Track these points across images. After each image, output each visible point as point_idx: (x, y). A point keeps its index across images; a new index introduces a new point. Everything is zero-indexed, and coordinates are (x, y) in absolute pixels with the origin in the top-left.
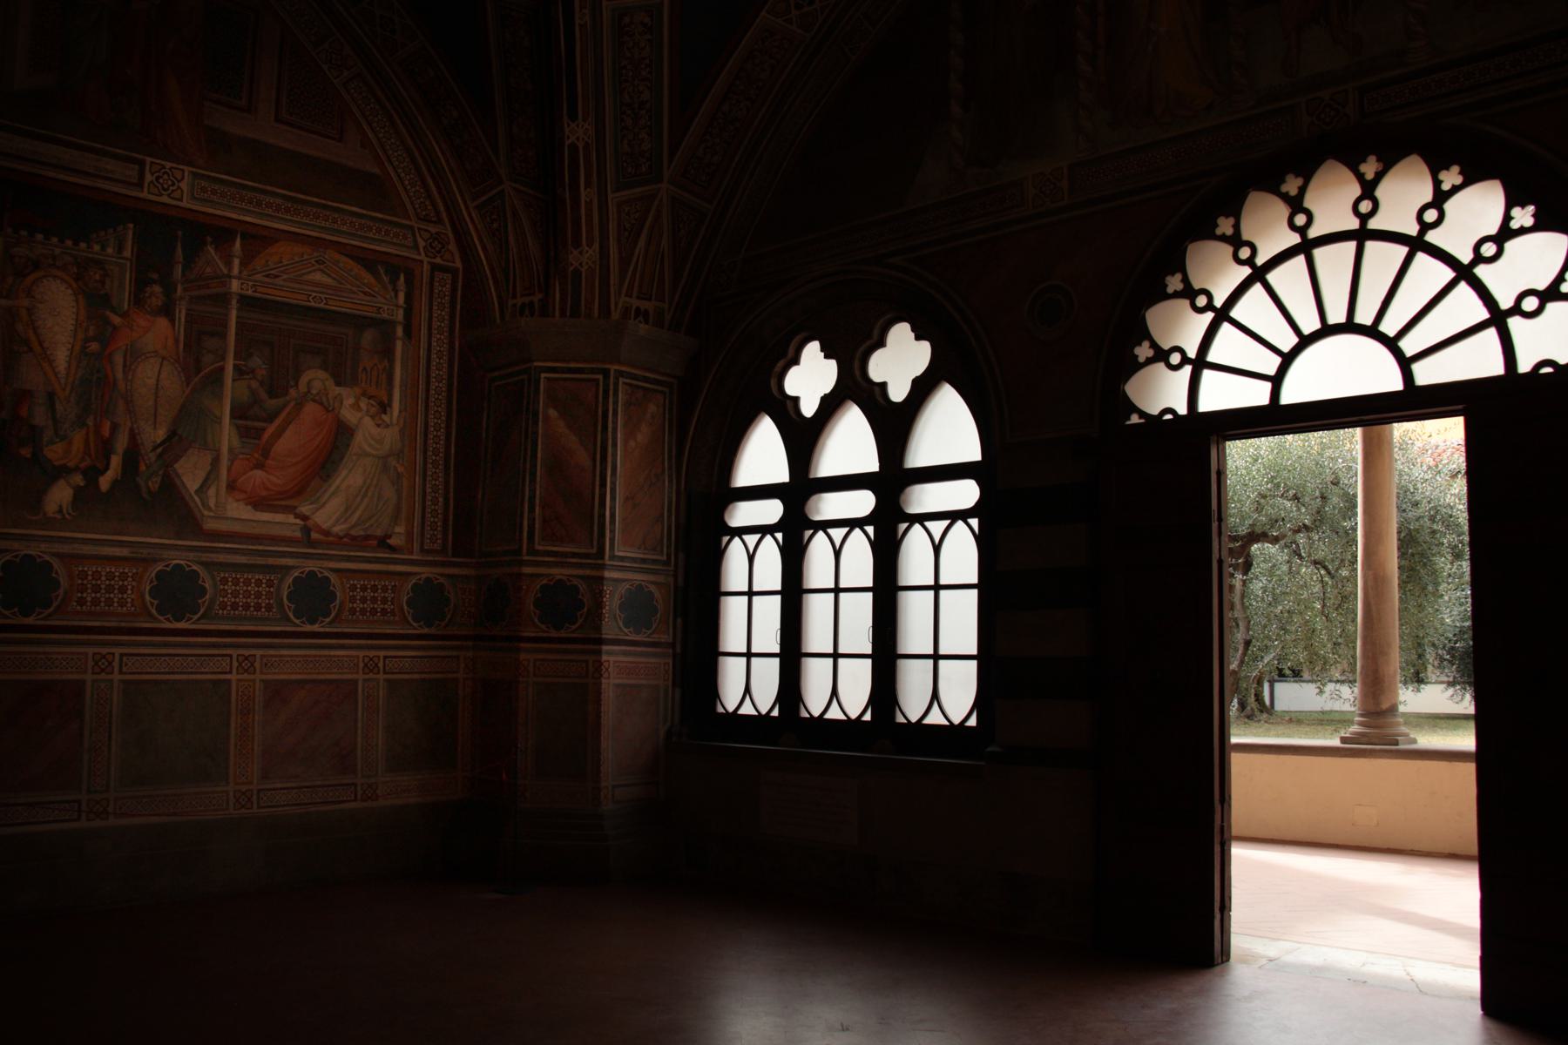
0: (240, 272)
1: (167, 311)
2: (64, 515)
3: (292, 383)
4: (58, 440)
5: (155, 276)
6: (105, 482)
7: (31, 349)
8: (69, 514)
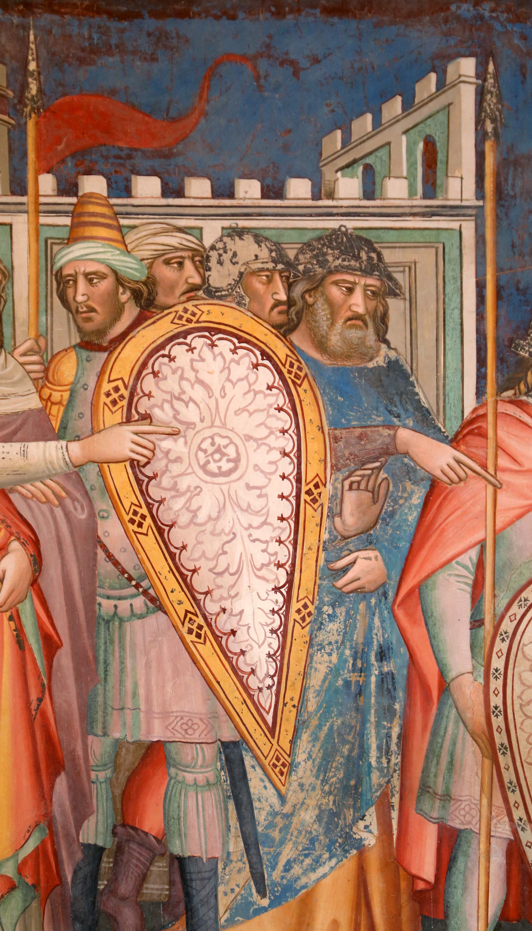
4: (265, 902)
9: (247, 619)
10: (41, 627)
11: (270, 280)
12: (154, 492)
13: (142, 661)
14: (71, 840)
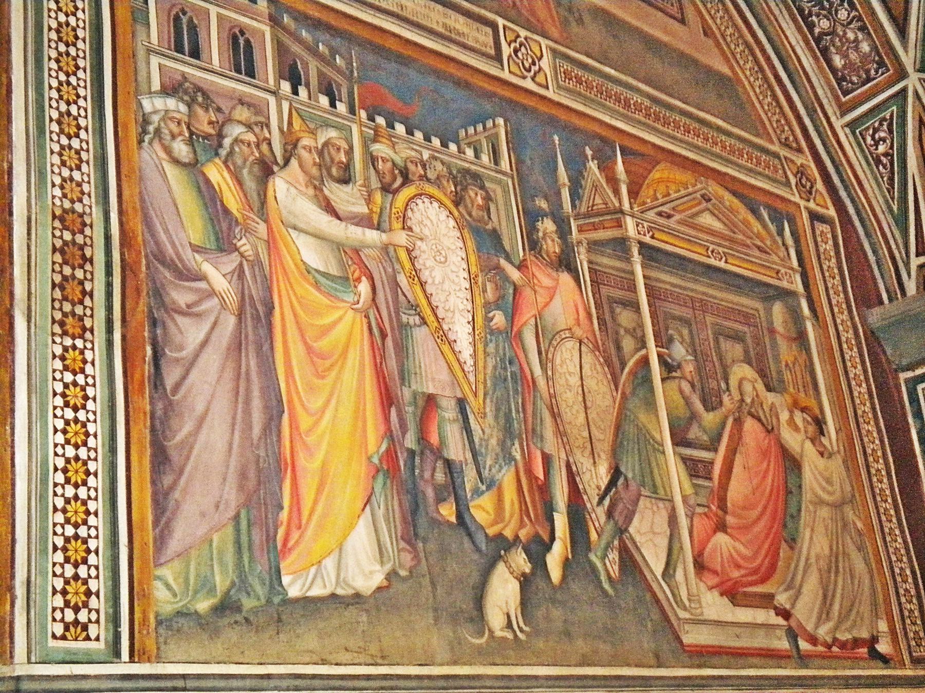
0: (632, 208)
1: (566, 263)
2: (516, 636)
3: (723, 385)
5: (544, 205)
6: (554, 560)
7: (424, 322)
8: (521, 630)
9: (459, 335)
10: (378, 324)
11: (448, 181)
12: (418, 266)
13: (421, 350)
14: (402, 445)
